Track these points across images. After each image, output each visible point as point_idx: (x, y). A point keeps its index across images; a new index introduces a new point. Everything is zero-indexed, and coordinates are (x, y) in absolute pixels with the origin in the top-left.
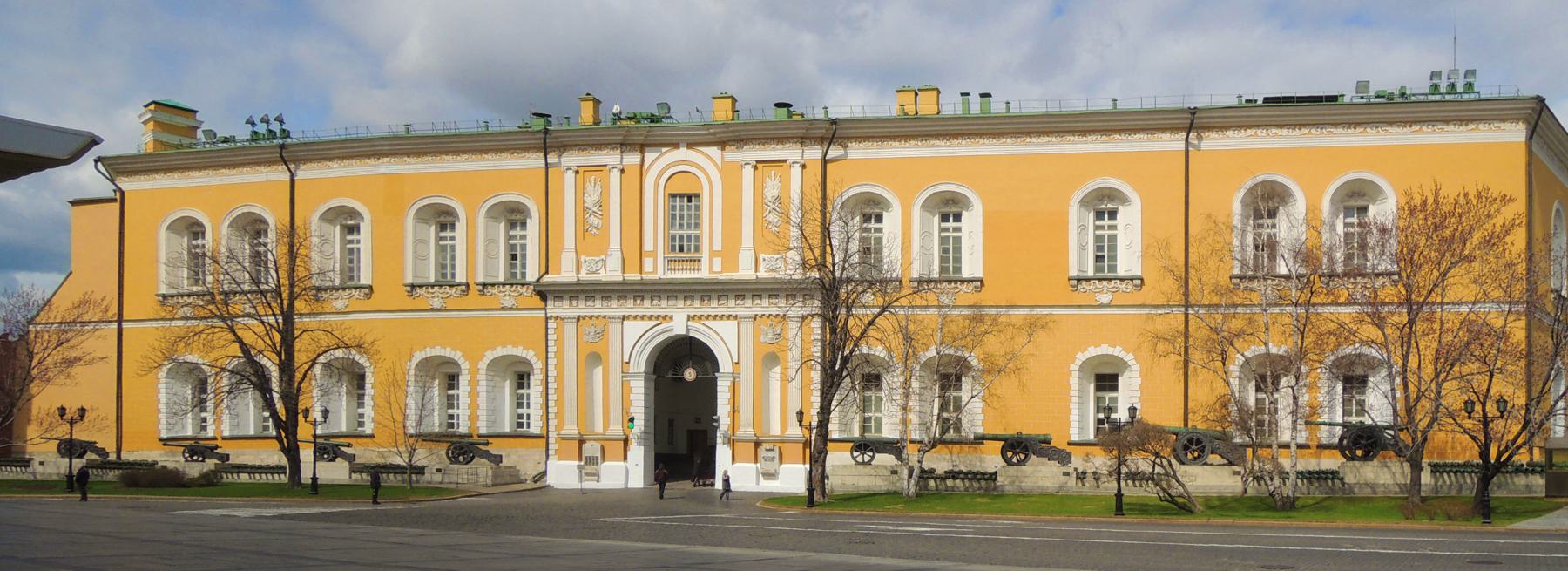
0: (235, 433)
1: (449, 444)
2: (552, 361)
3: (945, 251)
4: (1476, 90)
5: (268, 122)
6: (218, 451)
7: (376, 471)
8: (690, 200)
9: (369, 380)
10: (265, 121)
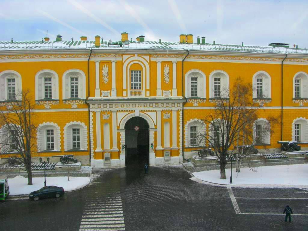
2: (92, 126)
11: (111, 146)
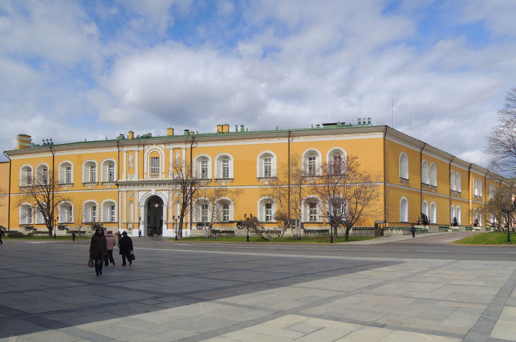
0: (39, 223)
1: (92, 225)
2: (120, 203)
3: (224, 171)
4: (371, 123)
5: (48, 141)
6: (34, 228)
7: (74, 233)
8: (156, 159)
9: (73, 208)
10: (47, 140)
11: (134, 219)
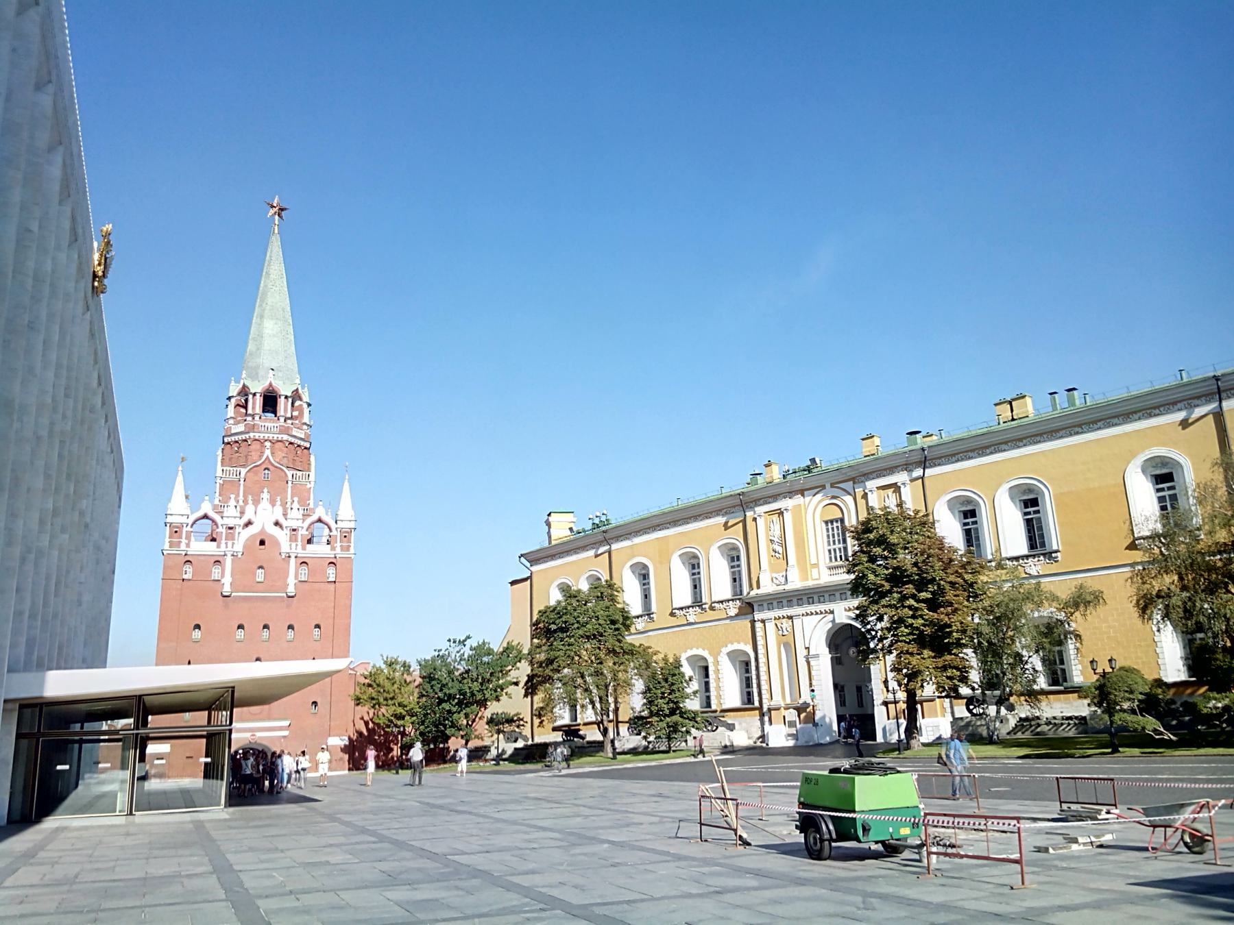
2: (761, 651)
